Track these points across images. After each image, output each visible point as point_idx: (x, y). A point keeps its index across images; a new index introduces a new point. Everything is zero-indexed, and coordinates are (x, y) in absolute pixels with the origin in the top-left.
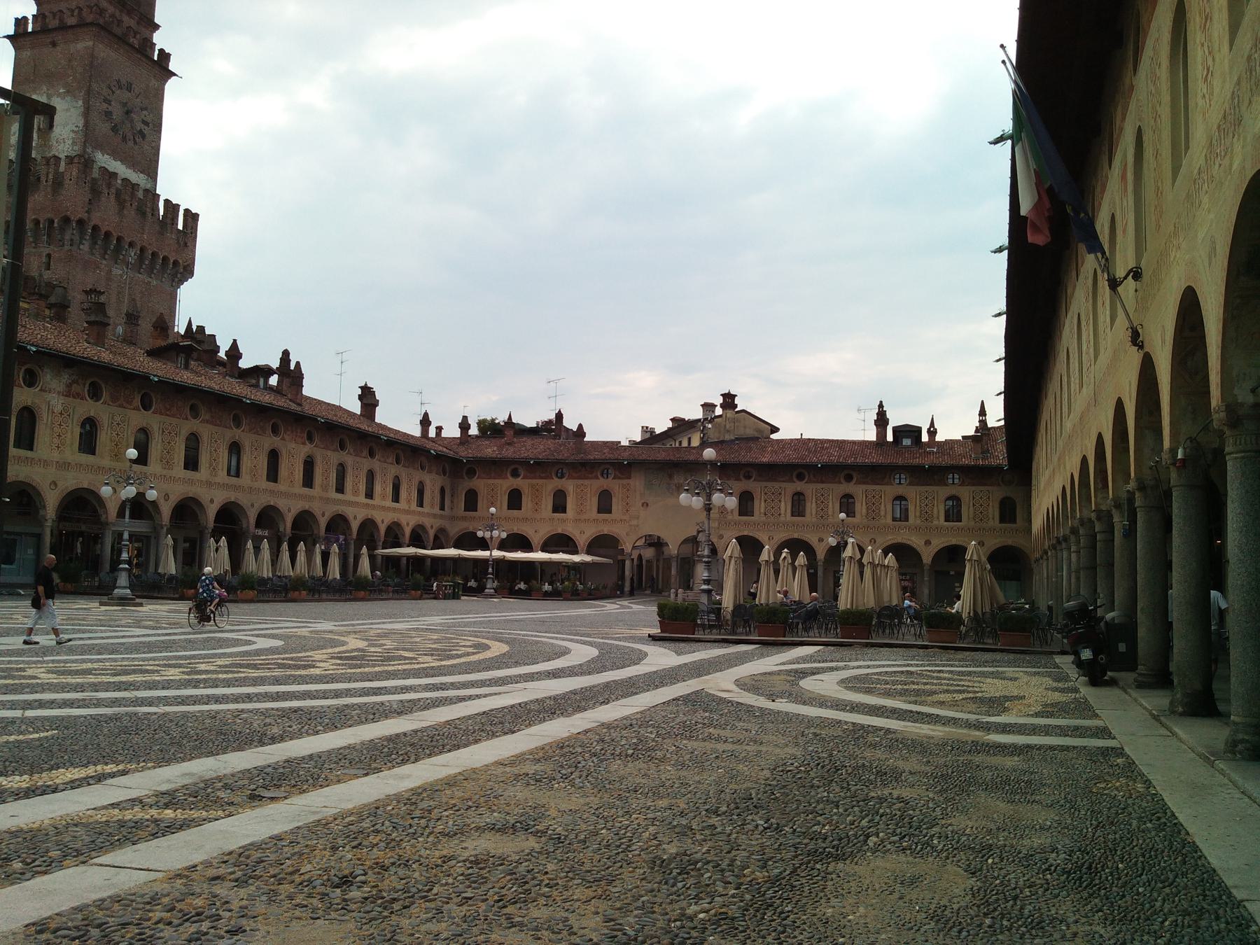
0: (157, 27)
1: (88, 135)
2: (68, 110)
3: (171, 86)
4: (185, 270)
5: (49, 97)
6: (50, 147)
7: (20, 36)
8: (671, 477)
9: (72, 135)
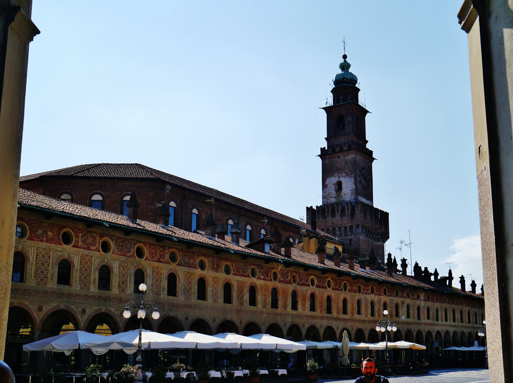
0: (367, 142)
3: (374, 164)
4: (386, 236)
5: (339, 177)
6: (342, 197)
7: (324, 154)
9: (351, 192)
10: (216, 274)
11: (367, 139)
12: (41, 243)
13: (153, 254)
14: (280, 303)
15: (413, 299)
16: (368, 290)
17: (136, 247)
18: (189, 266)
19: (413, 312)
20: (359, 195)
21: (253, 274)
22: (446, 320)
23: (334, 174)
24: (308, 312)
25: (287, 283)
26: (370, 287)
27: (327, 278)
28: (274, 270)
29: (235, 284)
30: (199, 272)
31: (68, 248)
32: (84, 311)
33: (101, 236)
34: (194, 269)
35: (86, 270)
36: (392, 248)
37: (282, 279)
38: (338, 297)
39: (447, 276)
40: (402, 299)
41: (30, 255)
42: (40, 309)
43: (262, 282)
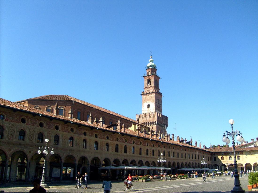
0: (160, 89)
3: (162, 98)
8: (250, 153)
10: (91, 138)
11: (160, 88)
12: (11, 122)
13: (63, 128)
14: (119, 150)
15: (176, 149)
16: (157, 146)
17: (55, 125)
18: (79, 134)
19: (176, 155)
21: (108, 138)
22: (189, 158)
24: (132, 154)
25: (122, 142)
26: (158, 145)
27: (140, 140)
28: (117, 137)
29: (99, 142)
30: (83, 137)
31: (24, 125)
32: (30, 152)
33: (40, 120)
34: (81, 135)
35: (32, 134)
36: (169, 130)
37: (120, 141)
38: (144, 149)
40: (171, 150)
41: (6, 127)
42: (10, 150)
43: (111, 142)
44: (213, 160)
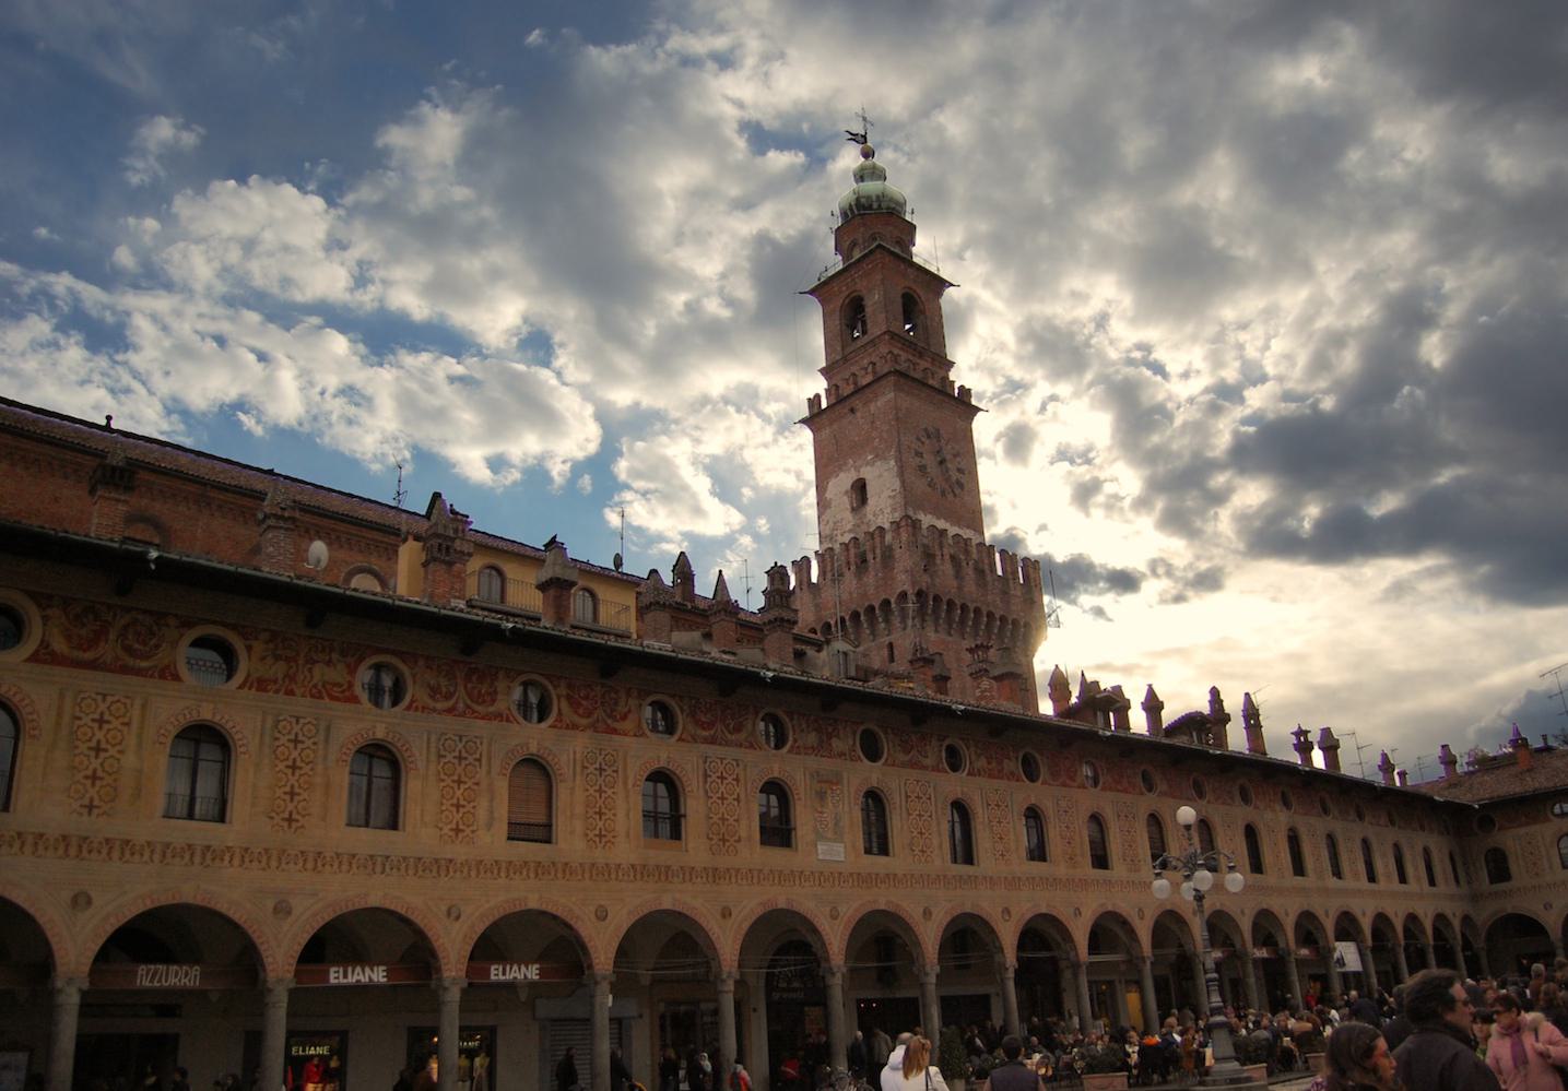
0: (951, 364)
1: (908, 497)
2: (880, 476)
5: (857, 470)
9: (890, 501)
15: (913, 765)
20: (920, 507)
23: (845, 464)
39: (1205, 709)
44: (1484, 874)
